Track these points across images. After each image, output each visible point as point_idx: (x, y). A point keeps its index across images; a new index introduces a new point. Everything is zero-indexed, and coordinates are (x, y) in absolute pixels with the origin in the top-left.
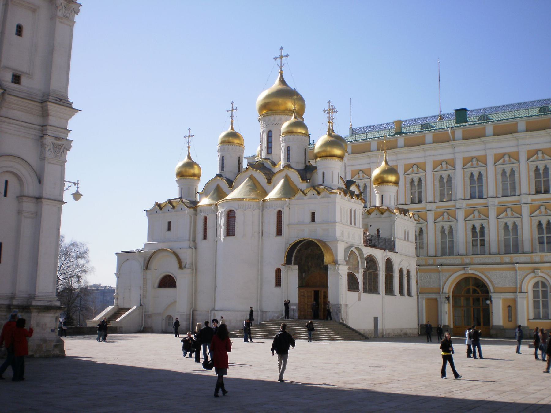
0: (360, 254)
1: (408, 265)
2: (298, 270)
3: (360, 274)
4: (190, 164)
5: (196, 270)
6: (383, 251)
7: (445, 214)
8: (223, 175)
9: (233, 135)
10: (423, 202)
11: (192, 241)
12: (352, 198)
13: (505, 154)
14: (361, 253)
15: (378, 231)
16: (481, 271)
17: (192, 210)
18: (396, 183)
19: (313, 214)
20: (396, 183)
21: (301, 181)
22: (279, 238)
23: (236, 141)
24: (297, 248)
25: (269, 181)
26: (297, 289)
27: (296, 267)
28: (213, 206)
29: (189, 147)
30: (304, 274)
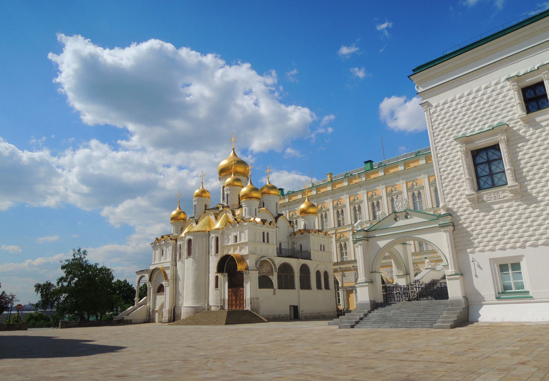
0: (272, 262)
3: (274, 276)
5: (176, 280)
6: (297, 259)
10: (345, 225)
11: (174, 261)
12: (264, 224)
14: (273, 262)
17: (174, 241)
19: (236, 237)
21: (233, 216)
23: (204, 195)
25: (216, 218)
27: (226, 274)
30: (233, 279)
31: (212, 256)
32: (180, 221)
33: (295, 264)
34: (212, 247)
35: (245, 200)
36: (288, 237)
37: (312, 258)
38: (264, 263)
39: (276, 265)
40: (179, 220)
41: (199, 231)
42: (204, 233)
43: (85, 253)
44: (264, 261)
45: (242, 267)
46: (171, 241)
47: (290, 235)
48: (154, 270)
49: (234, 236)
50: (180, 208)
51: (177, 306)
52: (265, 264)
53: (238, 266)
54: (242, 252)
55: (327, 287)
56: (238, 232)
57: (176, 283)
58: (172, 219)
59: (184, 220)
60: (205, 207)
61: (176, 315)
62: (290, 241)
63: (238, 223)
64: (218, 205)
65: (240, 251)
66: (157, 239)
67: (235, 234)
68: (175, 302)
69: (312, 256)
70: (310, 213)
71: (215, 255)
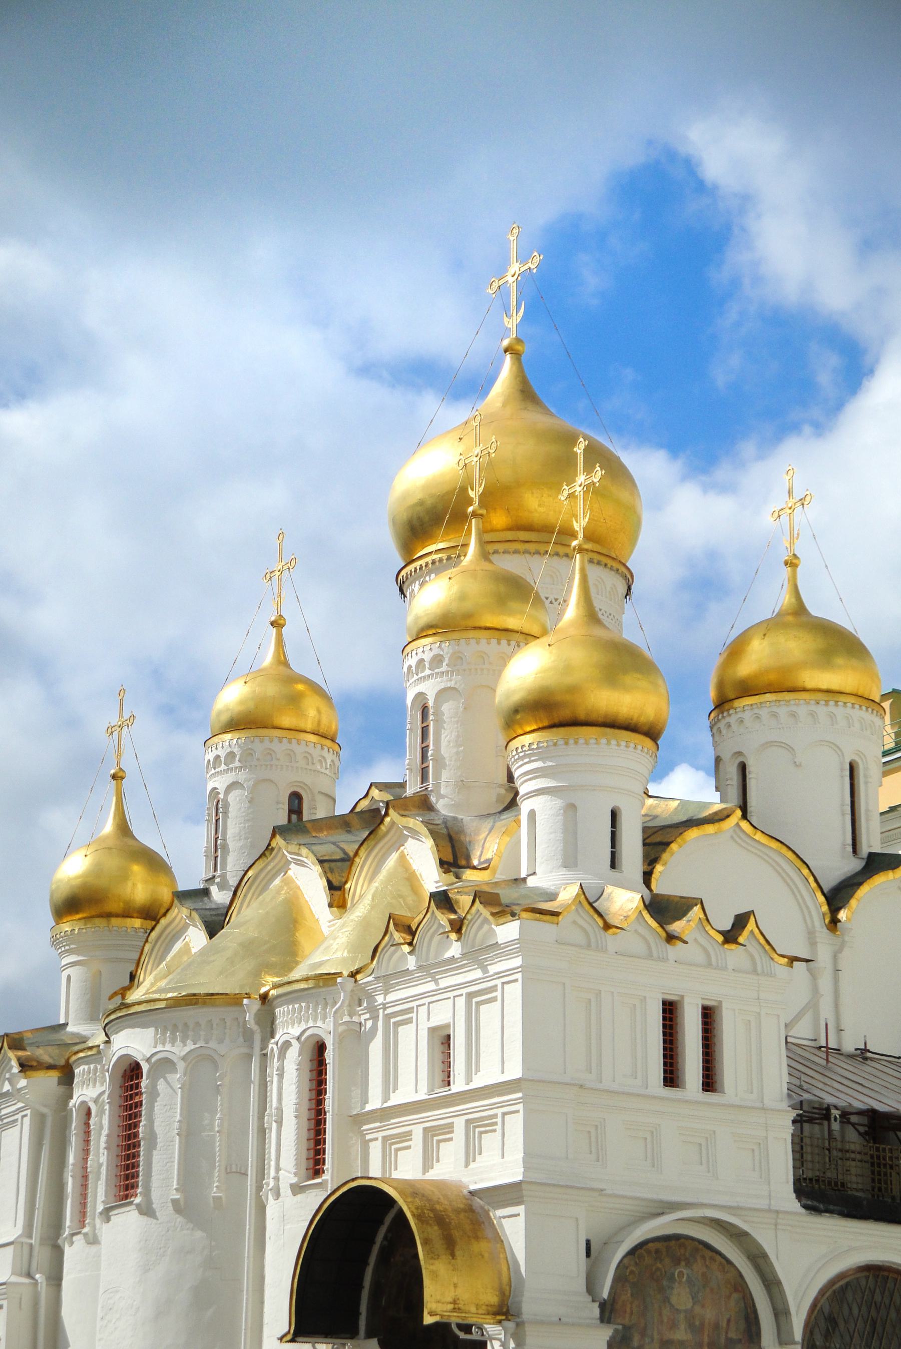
8: (214, 889)
31: (277, 1195)
32: (115, 921)
34: (280, 1123)
38: (677, 1262)
39: (779, 1283)
40: (109, 915)
45: (464, 1295)
46: (23, 1083)
49: (432, 1031)
54: (481, 1161)
56: (461, 1002)
60: (291, 811)
63: (459, 931)
64: (375, 793)
65: (471, 1153)
67: (441, 1015)
71: (297, 1189)
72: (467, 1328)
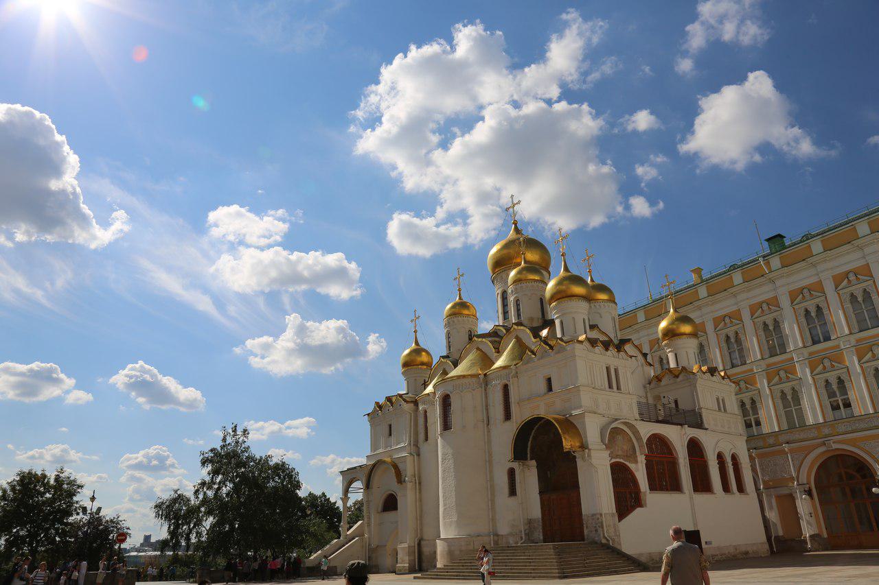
0: (633, 433)
1: (732, 447)
2: (537, 467)
3: (639, 464)
4: (418, 351)
5: (420, 483)
7: (782, 373)
9: (462, 305)
10: (748, 362)
11: (414, 445)
12: (607, 349)
13: (849, 272)
14: (636, 433)
15: (676, 402)
16: (853, 442)
18: (694, 335)
19: (549, 380)
20: (694, 335)
22: (508, 423)
23: (466, 312)
24: (533, 433)
26: (538, 497)
27: (534, 463)
28: (432, 395)
29: (415, 332)
30: (549, 472)
32: (420, 366)
33: (678, 437)
34: (493, 406)
35: (554, 304)
36: (645, 387)
37: (706, 426)
41: (464, 376)
42: (474, 380)
43: (245, 432)
44: (616, 431)
47: (647, 382)
48: (374, 466)
50: (417, 343)
51: (425, 537)
52: (620, 438)
53: (563, 440)
55: (741, 489)
57: (420, 489)
58: (406, 365)
59: (429, 365)
61: (424, 558)
62: (649, 395)
66: (379, 406)
68: (421, 530)
69: (705, 422)
70: (685, 334)
72: (574, 452)
